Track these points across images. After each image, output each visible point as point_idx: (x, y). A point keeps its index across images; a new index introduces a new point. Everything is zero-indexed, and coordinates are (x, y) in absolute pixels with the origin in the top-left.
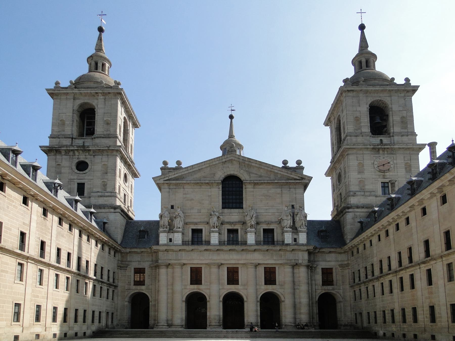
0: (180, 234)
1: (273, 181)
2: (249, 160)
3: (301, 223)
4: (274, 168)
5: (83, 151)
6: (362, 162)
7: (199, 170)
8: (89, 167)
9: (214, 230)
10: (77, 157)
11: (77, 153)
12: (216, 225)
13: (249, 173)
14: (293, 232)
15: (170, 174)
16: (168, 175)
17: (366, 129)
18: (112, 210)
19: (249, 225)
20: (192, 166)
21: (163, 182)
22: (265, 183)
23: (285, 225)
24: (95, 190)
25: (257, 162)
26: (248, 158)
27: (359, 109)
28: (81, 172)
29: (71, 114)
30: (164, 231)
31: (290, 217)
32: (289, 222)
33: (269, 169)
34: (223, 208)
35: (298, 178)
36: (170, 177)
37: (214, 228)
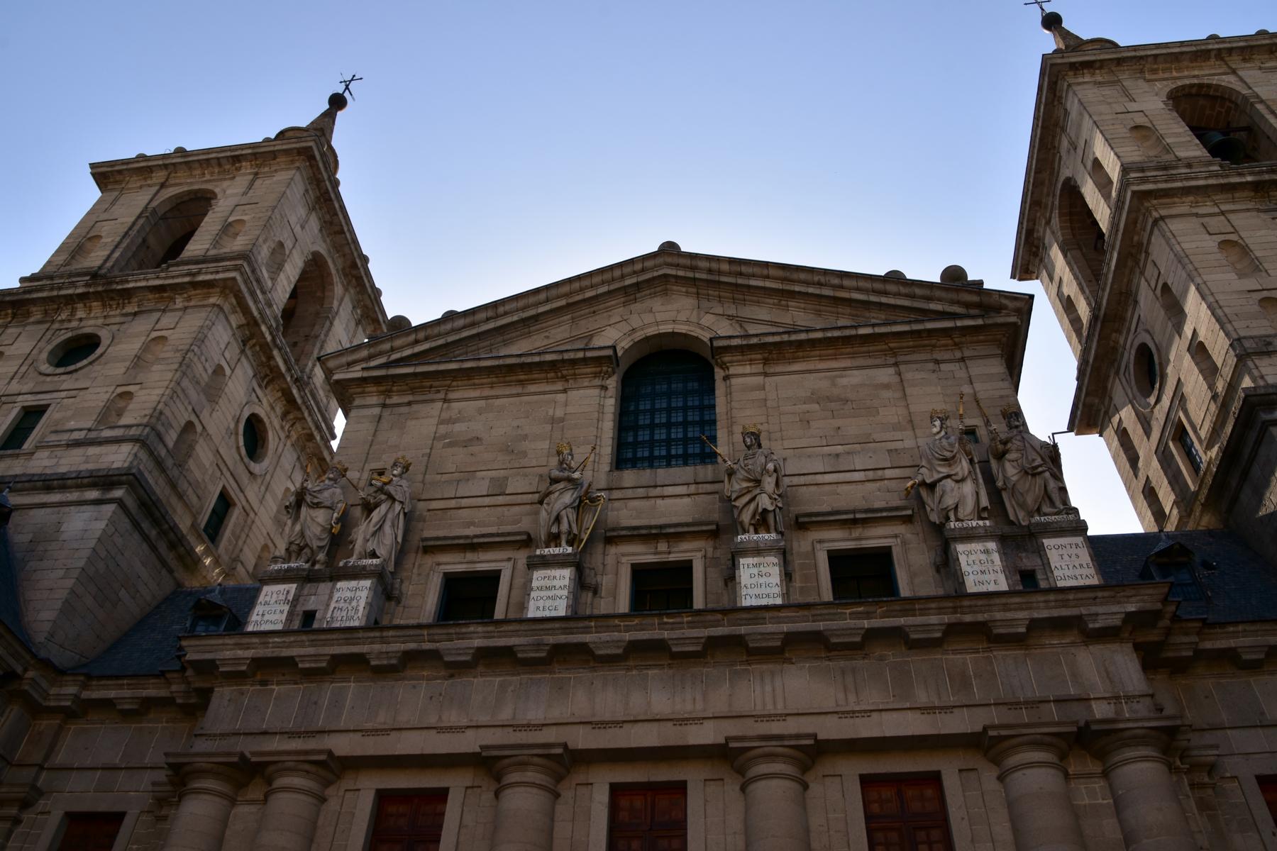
0: (367, 583)
1: (853, 332)
2: (736, 268)
3: (1038, 490)
4: (846, 282)
5: (104, 306)
6: (1233, 237)
7: (523, 321)
8: (99, 351)
9: (557, 551)
10: (74, 324)
11: (80, 314)
13: (741, 321)
14: (1003, 540)
15: (398, 343)
16: (387, 346)
17: (1193, 149)
18: (93, 494)
19: (746, 517)
20: (495, 305)
21: (359, 375)
22: (813, 343)
23: (949, 501)
24: (72, 424)
25: (772, 272)
27: (1133, 106)
28: (61, 370)
30: (289, 570)
31: (963, 467)
32: (968, 488)
33: (827, 292)
34: (620, 462)
36: (395, 356)
37: (558, 545)
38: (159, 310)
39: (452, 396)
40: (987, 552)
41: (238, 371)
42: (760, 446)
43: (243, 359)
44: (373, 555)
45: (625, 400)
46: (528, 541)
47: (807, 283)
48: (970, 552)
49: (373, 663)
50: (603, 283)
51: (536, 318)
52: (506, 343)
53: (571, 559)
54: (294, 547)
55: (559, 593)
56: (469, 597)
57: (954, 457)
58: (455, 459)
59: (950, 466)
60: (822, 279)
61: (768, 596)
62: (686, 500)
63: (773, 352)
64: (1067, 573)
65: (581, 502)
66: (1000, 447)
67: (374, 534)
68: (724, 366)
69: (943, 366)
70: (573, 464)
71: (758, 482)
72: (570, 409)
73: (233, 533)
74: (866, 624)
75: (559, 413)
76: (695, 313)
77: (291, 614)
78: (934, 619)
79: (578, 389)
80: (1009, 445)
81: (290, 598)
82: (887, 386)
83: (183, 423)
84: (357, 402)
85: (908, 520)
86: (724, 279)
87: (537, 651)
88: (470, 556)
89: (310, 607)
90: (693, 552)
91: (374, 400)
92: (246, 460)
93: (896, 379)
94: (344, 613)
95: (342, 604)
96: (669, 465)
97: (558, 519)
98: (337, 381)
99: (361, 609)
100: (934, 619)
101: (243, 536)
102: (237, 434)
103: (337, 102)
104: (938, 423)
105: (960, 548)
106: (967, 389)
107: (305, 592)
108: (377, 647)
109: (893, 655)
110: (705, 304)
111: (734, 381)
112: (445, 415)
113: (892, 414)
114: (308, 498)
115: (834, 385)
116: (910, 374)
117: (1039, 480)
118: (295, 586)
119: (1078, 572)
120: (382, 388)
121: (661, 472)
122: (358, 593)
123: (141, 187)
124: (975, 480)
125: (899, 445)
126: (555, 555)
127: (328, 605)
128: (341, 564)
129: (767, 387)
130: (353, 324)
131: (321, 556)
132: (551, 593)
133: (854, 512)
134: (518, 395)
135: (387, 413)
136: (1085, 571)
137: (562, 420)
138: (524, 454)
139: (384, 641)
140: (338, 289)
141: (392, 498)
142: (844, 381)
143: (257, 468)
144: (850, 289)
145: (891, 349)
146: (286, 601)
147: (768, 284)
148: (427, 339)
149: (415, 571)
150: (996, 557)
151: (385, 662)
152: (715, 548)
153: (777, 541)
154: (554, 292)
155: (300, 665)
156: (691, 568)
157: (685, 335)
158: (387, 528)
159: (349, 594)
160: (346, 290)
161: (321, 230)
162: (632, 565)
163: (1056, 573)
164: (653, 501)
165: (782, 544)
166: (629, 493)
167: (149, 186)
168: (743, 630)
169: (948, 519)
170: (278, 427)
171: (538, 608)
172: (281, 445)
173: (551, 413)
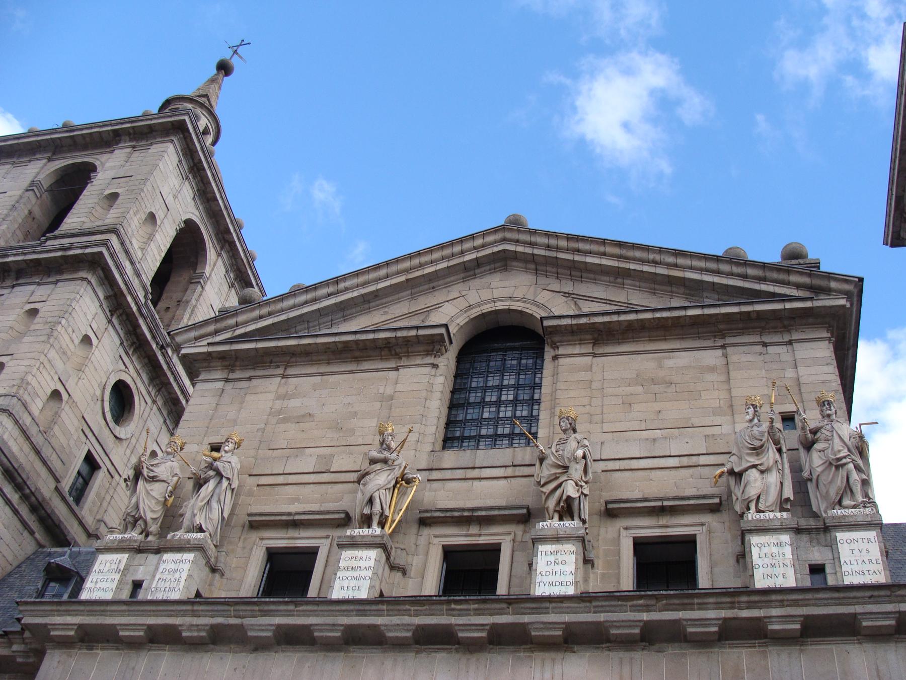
0: (190, 556)
1: (682, 313)
2: (574, 245)
3: (840, 482)
4: (681, 261)
12: (377, 508)
15: (241, 318)
16: (232, 321)
19: (551, 504)
23: (752, 492)
25: (609, 249)
26: (569, 237)
29: (19, 193)
30: (122, 541)
31: (771, 455)
35: (794, 292)
36: (239, 332)
38: (34, 283)
39: (291, 371)
40: (780, 545)
41: (106, 340)
42: (575, 431)
43: (110, 328)
44: (201, 530)
45: (461, 375)
46: (346, 521)
47: (643, 261)
48: (763, 545)
49: (184, 634)
50: (443, 258)
51: (376, 295)
52: (345, 319)
53: (378, 541)
54: (129, 519)
55: (364, 573)
56: (288, 574)
57: (762, 446)
58: (288, 434)
59: (758, 455)
60: (657, 257)
61: (561, 584)
62: (503, 482)
63: (602, 335)
64: (856, 568)
65: (397, 482)
66: (809, 435)
67: (201, 509)
68: (555, 347)
69: (771, 349)
70: (393, 445)
71: (566, 468)
72: (400, 387)
73: (98, 494)
74: (645, 616)
75: (389, 391)
76: (532, 289)
77: (120, 582)
78: (711, 614)
79: (409, 366)
80: (819, 434)
81: (122, 567)
82: (712, 369)
83: (49, 392)
84: (202, 377)
85: (714, 509)
86: (561, 255)
87: (332, 631)
88: (292, 533)
89: (138, 577)
90: (503, 537)
91: (219, 375)
92: (112, 424)
93: (723, 361)
94: (167, 585)
95: (165, 576)
96: (493, 446)
97: (371, 501)
98: (185, 356)
99: (183, 580)
100: (711, 614)
101: (108, 498)
102: (103, 400)
103: (224, 68)
104: (751, 410)
105: (755, 540)
106: (790, 373)
107: (136, 563)
108: (188, 620)
109: (672, 650)
110: (542, 280)
111: (562, 361)
112: (282, 391)
113: (714, 398)
114: (145, 472)
115: (661, 367)
116: (737, 355)
117: (842, 473)
118: (127, 556)
119: (866, 567)
120: (226, 363)
121: (480, 453)
122: (182, 566)
123: (30, 161)
124: (781, 471)
125: (716, 431)
126: (363, 536)
127: (154, 576)
128: (169, 537)
129: (594, 368)
130: (226, 287)
131: (153, 528)
132: (355, 574)
133: (661, 499)
134: (353, 372)
135: (230, 385)
136: (872, 567)
137: (391, 398)
138: (352, 432)
139: (195, 614)
140: (211, 253)
141: (219, 475)
142: (670, 363)
143: (121, 431)
144: (684, 268)
145: (720, 331)
146: (118, 570)
147: (605, 262)
148: (270, 314)
149: (240, 544)
150: (788, 550)
151: (195, 634)
152: (525, 532)
153: (578, 529)
154: (394, 268)
155: (121, 633)
156: (499, 550)
157: (521, 312)
158: (215, 505)
159: (172, 566)
160: (219, 255)
161: (194, 198)
162: (443, 546)
163: (844, 568)
164: (470, 482)
165: (582, 532)
166: (448, 474)
167: (38, 159)
168: (526, 619)
169: (748, 509)
170: (144, 392)
171: (342, 588)
172: (148, 409)
173: (381, 391)
